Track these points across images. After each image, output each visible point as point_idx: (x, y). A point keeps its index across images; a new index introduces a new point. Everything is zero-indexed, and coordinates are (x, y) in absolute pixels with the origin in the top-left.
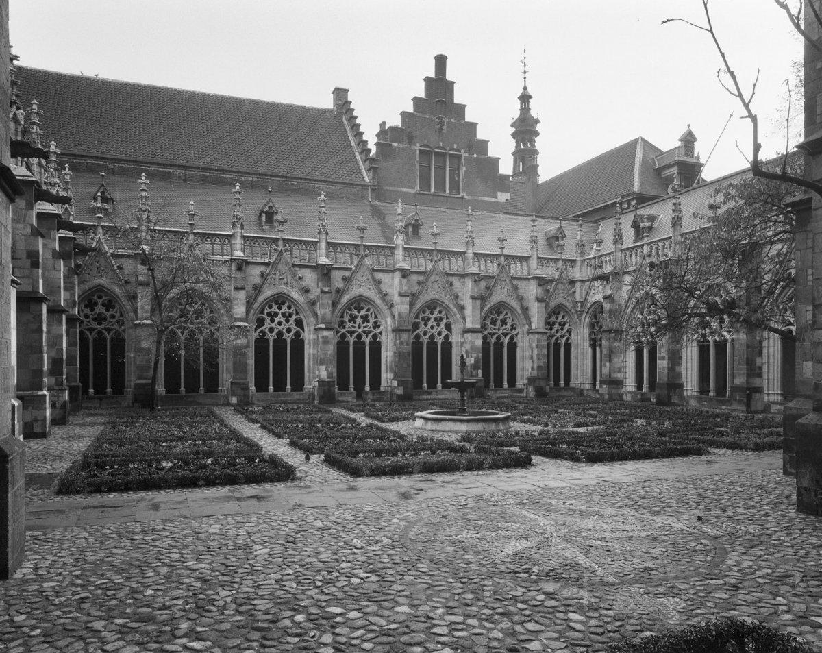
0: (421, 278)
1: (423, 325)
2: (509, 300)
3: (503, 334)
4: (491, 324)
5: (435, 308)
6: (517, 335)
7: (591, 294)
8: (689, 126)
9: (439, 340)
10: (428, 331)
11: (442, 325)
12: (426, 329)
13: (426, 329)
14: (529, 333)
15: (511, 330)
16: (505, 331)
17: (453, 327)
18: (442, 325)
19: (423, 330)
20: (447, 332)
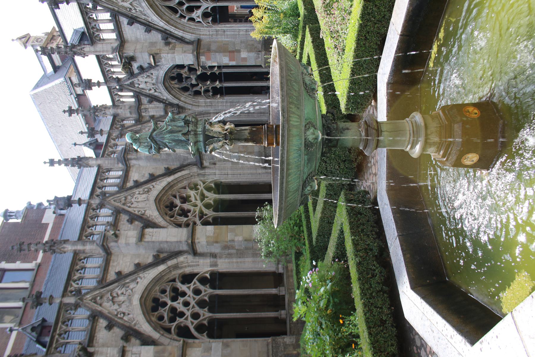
0: (103, 323)
1: (182, 320)
2: (155, 193)
3: (202, 200)
4: (187, 216)
5: (156, 300)
6: (204, 183)
7: (156, 94)
8: (13, 40)
9: (207, 291)
10: (190, 311)
11: (183, 288)
12: (188, 314)
13: (188, 314)
14: (202, 167)
15: (197, 189)
16: (198, 198)
17: (188, 270)
18: (183, 288)
19: (190, 319)
20: (195, 280)
